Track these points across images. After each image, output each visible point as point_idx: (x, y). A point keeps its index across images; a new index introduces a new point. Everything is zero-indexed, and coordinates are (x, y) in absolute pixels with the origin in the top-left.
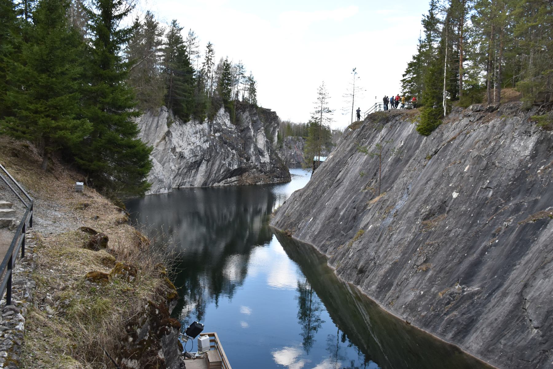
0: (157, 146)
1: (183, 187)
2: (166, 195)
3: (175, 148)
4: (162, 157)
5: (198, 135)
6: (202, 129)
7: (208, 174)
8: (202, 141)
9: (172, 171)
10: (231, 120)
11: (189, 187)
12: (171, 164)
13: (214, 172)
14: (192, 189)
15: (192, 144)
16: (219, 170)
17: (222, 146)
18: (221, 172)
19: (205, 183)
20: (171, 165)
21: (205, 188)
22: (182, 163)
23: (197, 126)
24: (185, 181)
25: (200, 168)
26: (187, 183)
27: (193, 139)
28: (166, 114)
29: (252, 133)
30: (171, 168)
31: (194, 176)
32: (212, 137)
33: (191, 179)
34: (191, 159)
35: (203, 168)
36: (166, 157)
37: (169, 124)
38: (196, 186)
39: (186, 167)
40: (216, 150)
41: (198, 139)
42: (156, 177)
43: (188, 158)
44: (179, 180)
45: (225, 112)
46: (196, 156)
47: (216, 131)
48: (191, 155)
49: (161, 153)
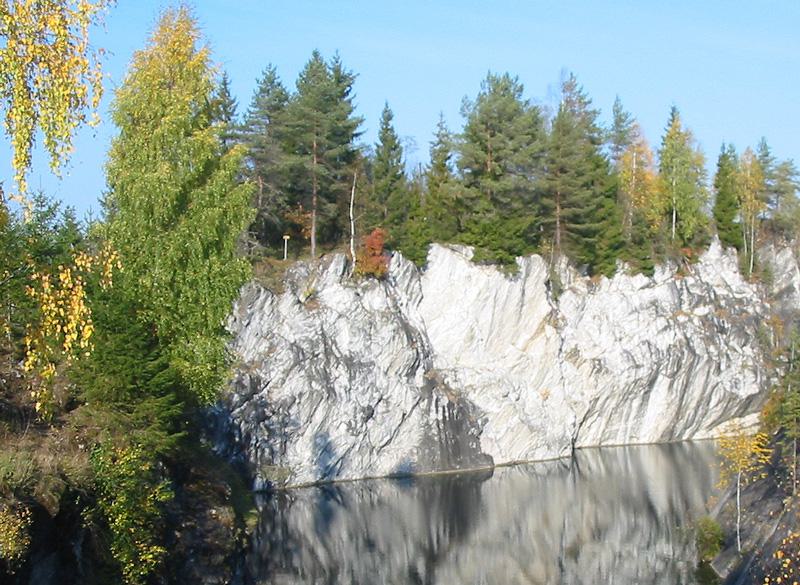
1: (610, 442)
6: (654, 303)
8: (654, 328)
13: (693, 405)
16: (704, 400)
17: (709, 340)
18: (712, 404)
19: (671, 432)
21: (669, 447)
22: (600, 387)
24: (615, 428)
25: (652, 395)
33: (631, 423)
34: (626, 374)
40: (692, 351)
46: (638, 367)
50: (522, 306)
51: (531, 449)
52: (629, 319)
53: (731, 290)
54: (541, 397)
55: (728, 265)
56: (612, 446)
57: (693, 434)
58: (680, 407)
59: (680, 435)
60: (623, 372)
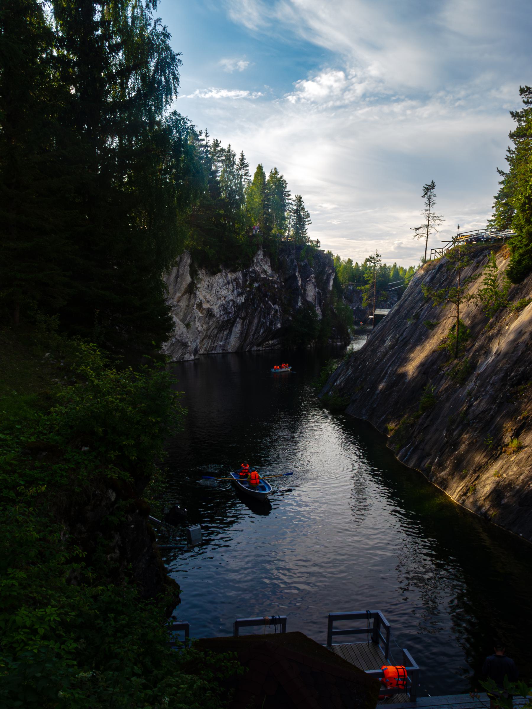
0: (178, 301)
1: (213, 352)
2: (192, 363)
3: (201, 303)
4: (185, 315)
5: (230, 287)
6: (236, 279)
7: (244, 336)
9: (199, 332)
10: (272, 267)
11: (221, 352)
12: (198, 324)
13: (252, 333)
14: (225, 354)
15: (222, 299)
16: (257, 331)
20: (197, 326)
21: (239, 353)
22: (211, 323)
23: (229, 275)
25: (234, 328)
26: (218, 348)
27: (224, 292)
28: (189, 261)
29: (300, 283)
30: (197, 328)
31: (226, 339)
32: (248, 289)
34: (222, 317)
35: (237, 328)
36: (190, 315)
37: (193, 273)
38: (230, 351)
39: (216, 327)
41: (230, 292)
42: (178, 340)
43: (218, 316)
44: (208, 343)
45: (264, 256)
47: (253, 280)
48: (222, 312)
49: (184, 310)
50: (178, 277)
51: (182, 355)
52: (224, 288)
53: (267, 275)
54: (186, 328)
55: (266, 262)
56: (214, 354)
57: (251, 348)
58: (246, 334)
59: (246, 349)
60: (221, 316)
